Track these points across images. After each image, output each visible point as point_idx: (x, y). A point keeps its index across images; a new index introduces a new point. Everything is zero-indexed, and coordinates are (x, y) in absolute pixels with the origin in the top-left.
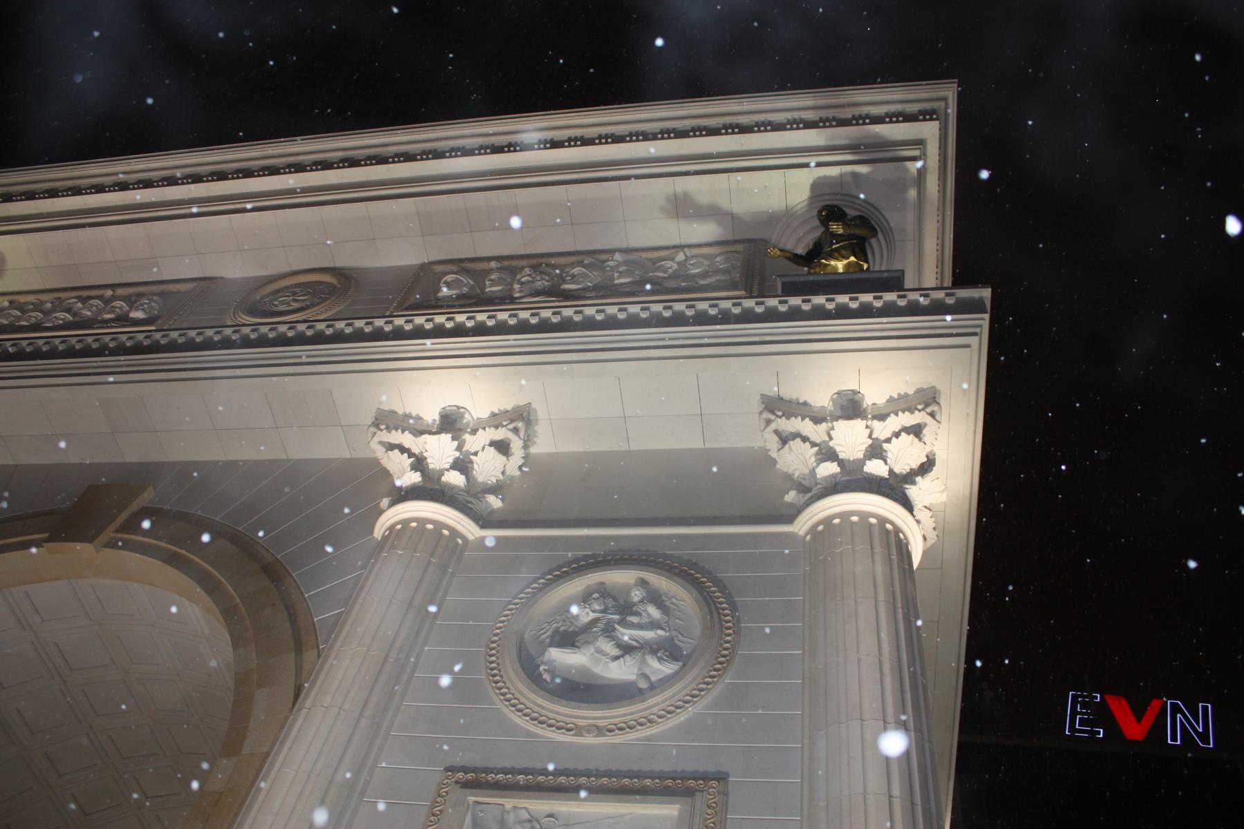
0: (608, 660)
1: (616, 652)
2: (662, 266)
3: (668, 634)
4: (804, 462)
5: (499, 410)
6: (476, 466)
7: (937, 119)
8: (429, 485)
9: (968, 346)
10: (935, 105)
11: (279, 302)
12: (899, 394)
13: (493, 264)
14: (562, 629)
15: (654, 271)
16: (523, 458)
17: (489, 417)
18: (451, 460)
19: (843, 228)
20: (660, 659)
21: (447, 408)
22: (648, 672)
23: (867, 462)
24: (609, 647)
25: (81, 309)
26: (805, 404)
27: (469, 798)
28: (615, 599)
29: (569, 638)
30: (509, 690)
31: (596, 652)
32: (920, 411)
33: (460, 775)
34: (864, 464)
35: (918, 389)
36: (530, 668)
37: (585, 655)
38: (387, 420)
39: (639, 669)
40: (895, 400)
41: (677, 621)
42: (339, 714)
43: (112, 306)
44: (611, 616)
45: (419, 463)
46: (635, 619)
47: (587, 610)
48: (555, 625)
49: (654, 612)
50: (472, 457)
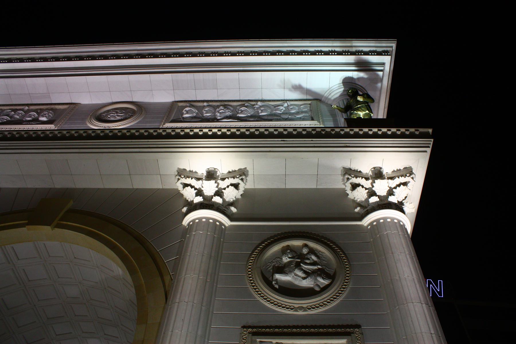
0: (300, 279)
1: (303, 275)
2: (279, 108)
3: (322, 267)
4: (362, 196)
5: (232, 170)
6: (225, 194)
7: (389, 55)
8: (206, 202)
9: (426, 152)
10: (388, 49)
11: (110, 116)
12: (397, 169)
13: (205, 104)
14: (276, 265)
15: (276, 111)
16: (243, 191)
17: (227, 173)
18: (214, 192)
19: (363, 99)
20: (323, 278)
21: (210, 169)
22: (319, 284)
23: (390, 197)
24: (300, 274)
25: (14, 115)
26: (360, 172)
27: (257, 340)
28: (296, 252)
29: (282, 269)
30: (261, 292)
31: (295, 275)
32: (408, 177)
33: (250, 330)
34: (388, 197)
35: (405, 167)
36: (269, 282)
37: (290, 277)
38: (182, 173)
39: (315, 283)
40: (395, 171)
41: (324, 261)
42: (193, 305)
43: (30, 115)
44: (297, 260)
45: (199, 193)
46: (308, 261)
47: (287, 257)
48: (273, 264)
49: (314, 258)
50: (223, 190)
